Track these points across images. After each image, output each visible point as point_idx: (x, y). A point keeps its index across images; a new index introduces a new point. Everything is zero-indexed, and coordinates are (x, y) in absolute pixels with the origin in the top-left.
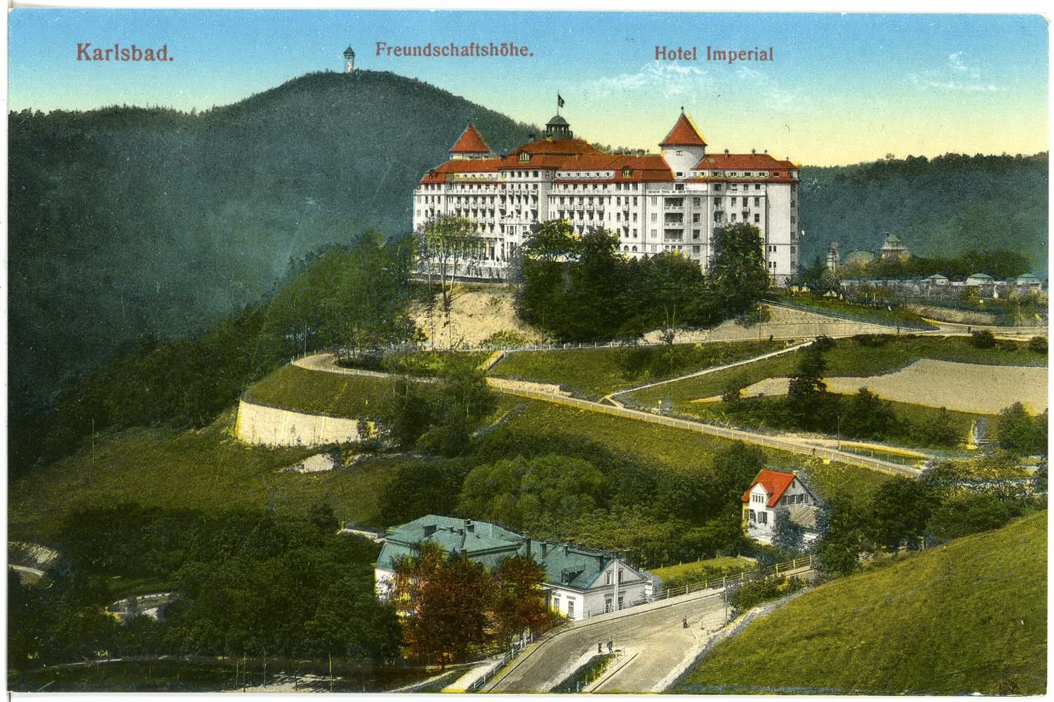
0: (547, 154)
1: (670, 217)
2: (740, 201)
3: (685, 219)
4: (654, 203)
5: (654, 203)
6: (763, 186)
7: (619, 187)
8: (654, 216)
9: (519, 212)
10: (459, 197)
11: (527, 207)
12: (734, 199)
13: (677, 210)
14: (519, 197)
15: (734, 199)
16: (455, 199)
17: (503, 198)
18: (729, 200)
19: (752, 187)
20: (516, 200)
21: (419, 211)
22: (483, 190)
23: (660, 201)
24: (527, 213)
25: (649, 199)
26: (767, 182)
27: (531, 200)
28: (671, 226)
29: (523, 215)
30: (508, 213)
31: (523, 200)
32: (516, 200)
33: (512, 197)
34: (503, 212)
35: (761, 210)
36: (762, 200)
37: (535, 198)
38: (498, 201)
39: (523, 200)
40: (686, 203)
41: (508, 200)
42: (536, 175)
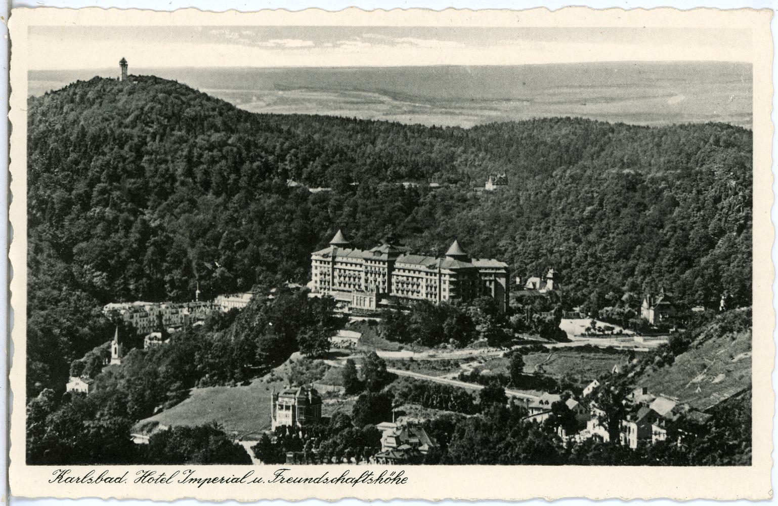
7: (427, 275)
8: (444, 290)
9: (375, 281)
10: (340, 270)
14: (375, 274)
16: (338, 270)
17: (366, 273)
20: (373, 275)
22: (353, 267)
30: (369, 281)
31: (377, 276)
32: (373, 275)
33: (371, 274)
34: (366, 281)
37: (384, 275)
38: (363, 275)
39: (377, 276)
42: (384, 264)
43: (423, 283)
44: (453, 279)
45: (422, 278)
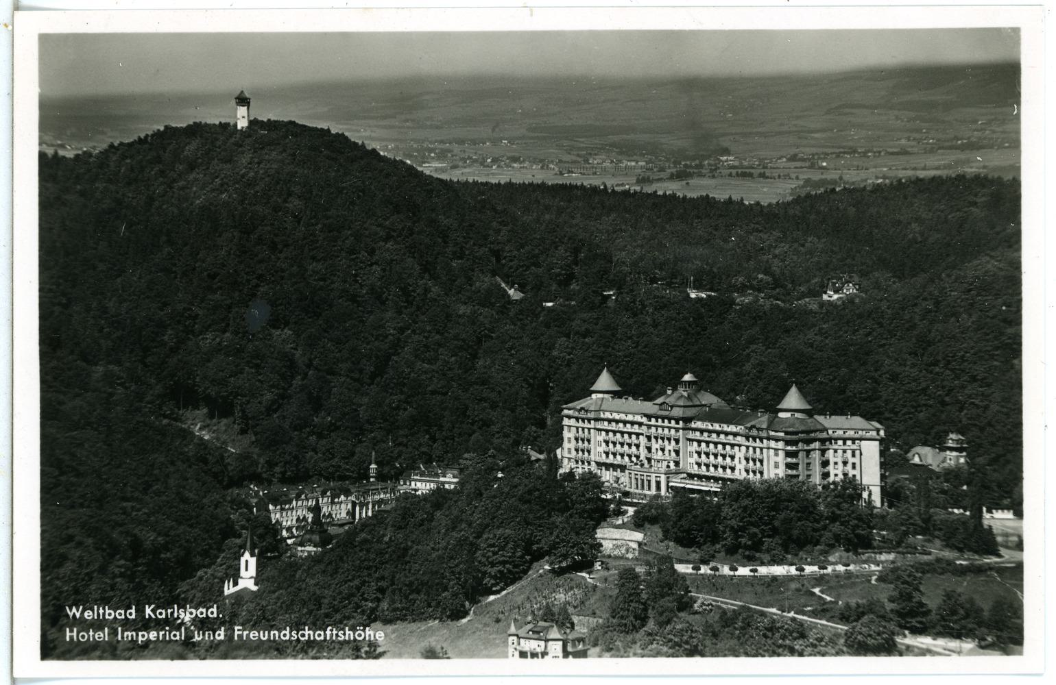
0: (685, 407)
1: (788, 466)
2: (840, 452)
3: (800, 467)
4: (777, 455)
5: (777, 455)
6: (857, 442)
11: (671, 446)
12: (836, 451)
13: (794, 461)
15: (836, 451)
17: (649, 438)
18: (831, 452)
19: (849, 443)
21: (569, 440)
23: (781, 454)
24: (670, 451)
25: (772, 451)
26: (861, 439)
27: (673, 443)
28: (790, 472)
29: (666, 452)
35: (857, 460)
36: (857, 453)
37: (677, 441)
40: (801, 454)
41: (653, 440)
43: (740, 453)
44: (789, 448)
45: (740, 446)
